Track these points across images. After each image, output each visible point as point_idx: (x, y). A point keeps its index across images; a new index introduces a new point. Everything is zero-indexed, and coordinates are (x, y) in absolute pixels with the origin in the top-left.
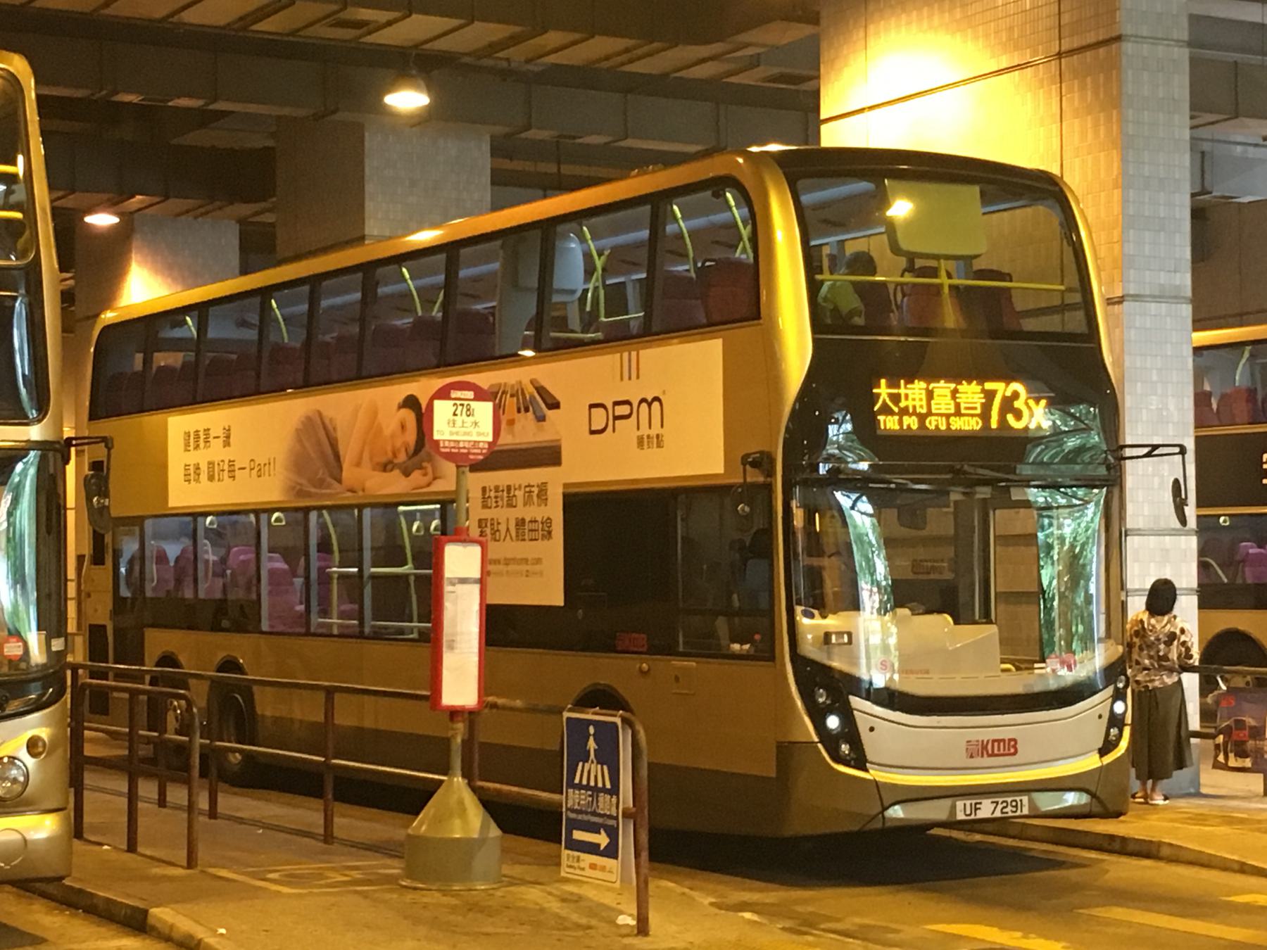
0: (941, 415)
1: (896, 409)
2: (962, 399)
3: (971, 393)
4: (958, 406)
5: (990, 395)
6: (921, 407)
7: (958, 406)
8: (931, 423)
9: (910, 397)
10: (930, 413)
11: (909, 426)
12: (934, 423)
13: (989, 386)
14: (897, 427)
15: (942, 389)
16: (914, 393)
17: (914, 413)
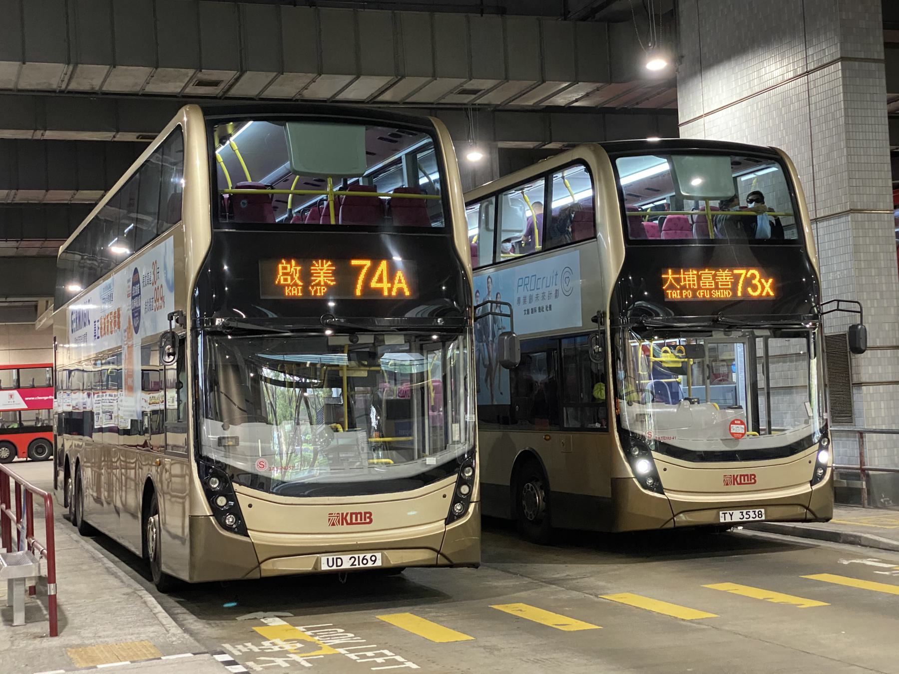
0: (707, 289)
6: (694, 285)
16: (689, 276)
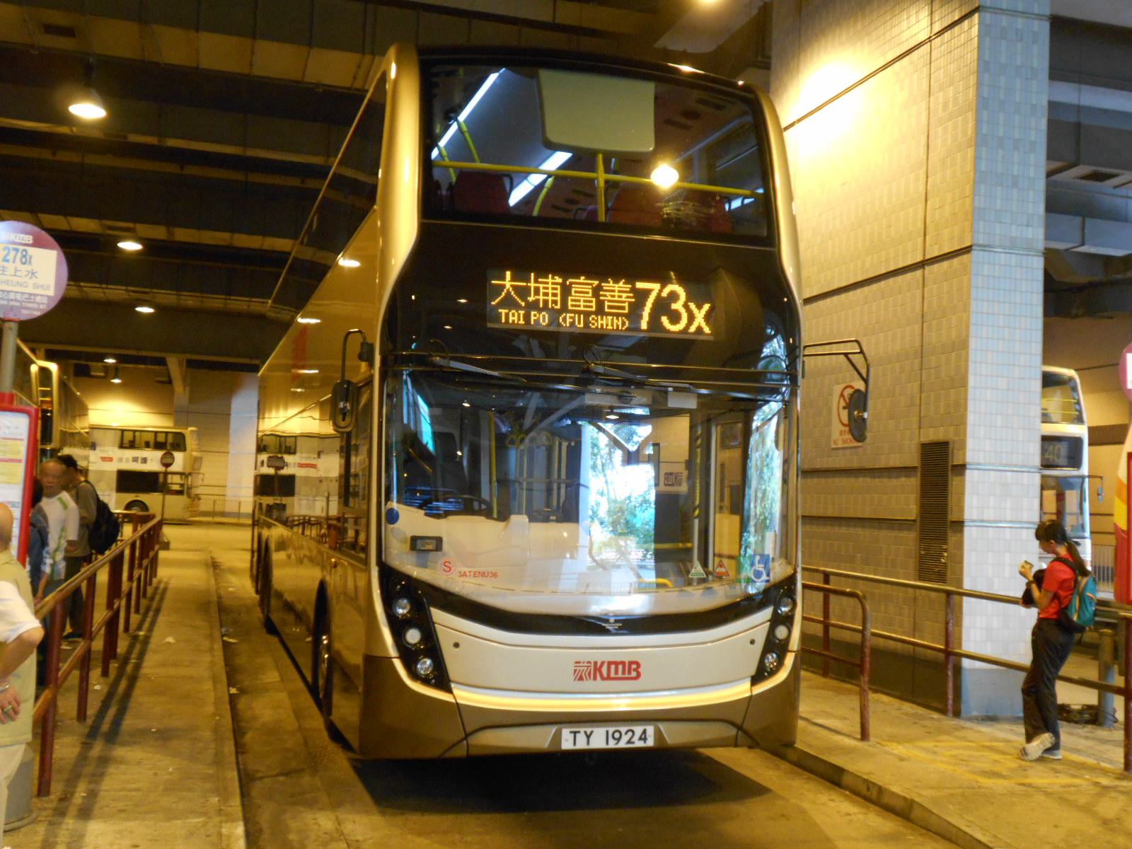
0: (579, 313)
1: (523, 304)
2: (606, 297)
3: (617, 291)
4: (600, 304)
5: (642, 296)
6: (555, 302)
7: (600, 304)
8: (566, 321)
9: (542, 291)
10: (564, 308)
11: (537, 321)
12: (569, 320)
13: (640, 285)
14: (522, 322)
15: (582, 288)
16: (547, 287)
17: (546, 308)
